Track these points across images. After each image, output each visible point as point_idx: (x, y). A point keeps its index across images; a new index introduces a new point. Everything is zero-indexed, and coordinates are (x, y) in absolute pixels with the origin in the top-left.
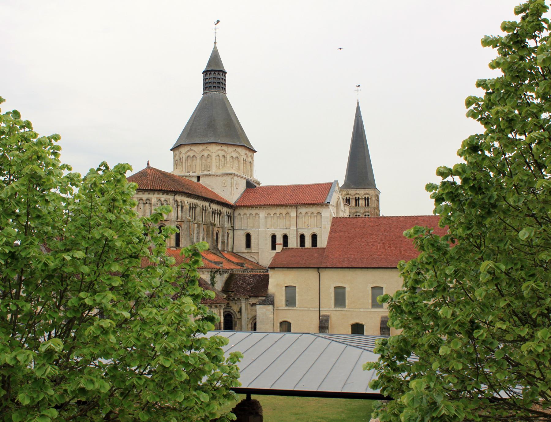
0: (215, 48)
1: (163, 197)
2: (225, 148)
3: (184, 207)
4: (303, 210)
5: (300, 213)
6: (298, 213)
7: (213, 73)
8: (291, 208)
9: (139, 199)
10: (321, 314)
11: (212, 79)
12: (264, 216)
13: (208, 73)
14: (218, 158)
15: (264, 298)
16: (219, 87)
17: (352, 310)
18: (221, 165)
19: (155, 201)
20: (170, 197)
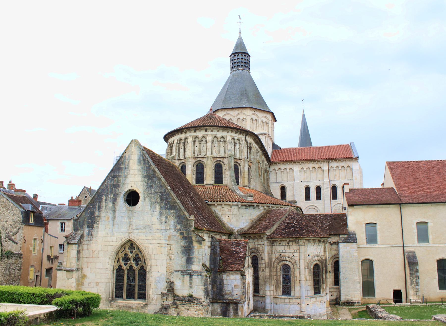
0: (240, 36)
1: (237, 136)
2: (257, 113)
3: (252, 149)
4: (334, 164)
5: (332, 167)
6: (330, 167)
7: (240, 54)
8: (322, 162)
9: (213, 136)
10: (405, 250)
11: (240, 59)
12: (298, 170)
13: (236, 55)
14: (251, 121)
15: (346, 236)
16: (246, 66)
17: (437, 245)
18: (254, 128)
19: (230, 139)
20: (242, 137)
